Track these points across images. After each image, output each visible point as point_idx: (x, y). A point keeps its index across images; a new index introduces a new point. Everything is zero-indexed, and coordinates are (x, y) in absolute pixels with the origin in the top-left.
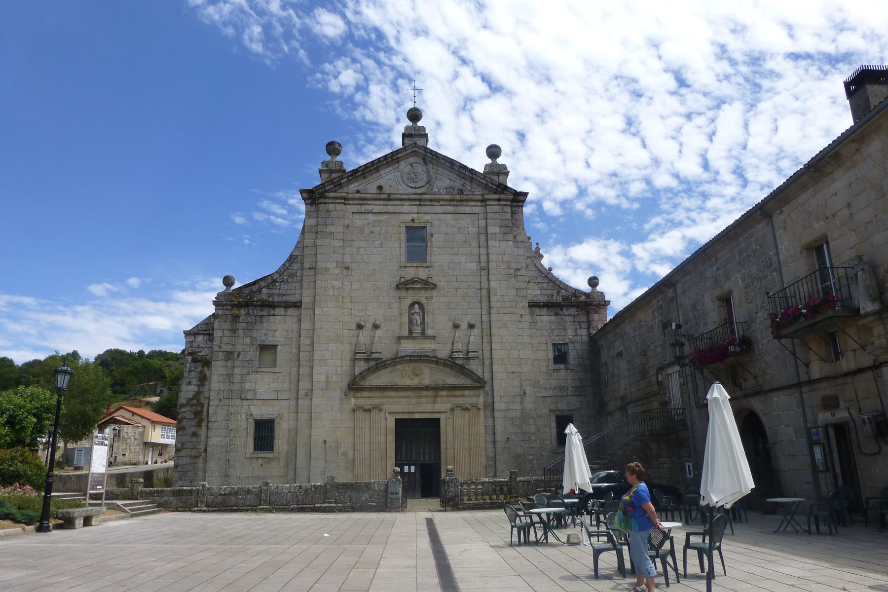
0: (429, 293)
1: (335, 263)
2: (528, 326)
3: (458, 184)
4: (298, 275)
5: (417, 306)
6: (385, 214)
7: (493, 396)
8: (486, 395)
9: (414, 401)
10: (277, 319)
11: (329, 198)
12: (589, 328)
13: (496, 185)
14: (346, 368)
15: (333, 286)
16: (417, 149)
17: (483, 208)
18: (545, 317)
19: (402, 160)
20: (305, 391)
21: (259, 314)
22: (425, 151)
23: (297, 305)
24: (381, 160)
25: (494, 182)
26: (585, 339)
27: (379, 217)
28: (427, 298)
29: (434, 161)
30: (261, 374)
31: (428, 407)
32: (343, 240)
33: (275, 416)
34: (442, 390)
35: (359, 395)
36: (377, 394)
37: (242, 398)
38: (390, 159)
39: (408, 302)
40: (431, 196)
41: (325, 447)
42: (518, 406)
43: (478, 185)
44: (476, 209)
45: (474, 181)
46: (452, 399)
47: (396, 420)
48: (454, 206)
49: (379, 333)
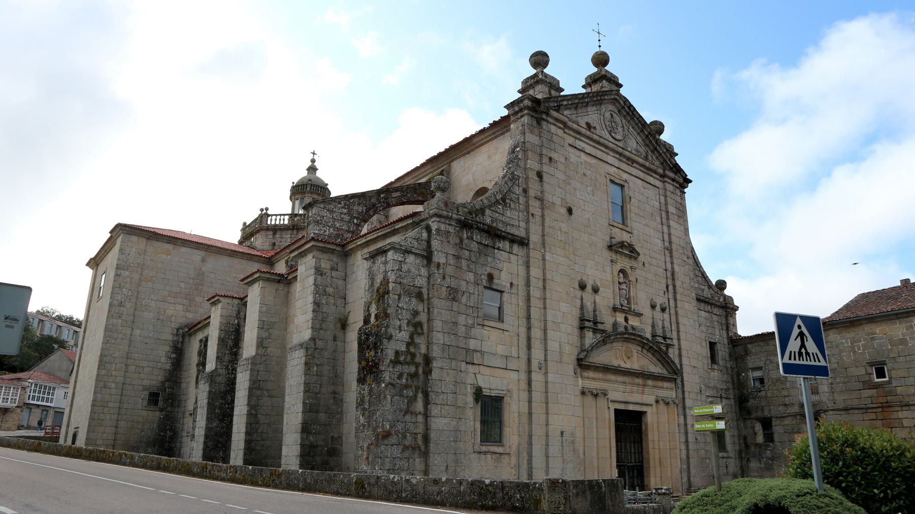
7: (683, 392)
10: (501, 254)
14: (575, 339)
20: (538, 361)
22: (624, 102)
23: (523, 242)
25: (672, 160)
26: (726, 341)
28: (631, 268)
29: (628, 118)
31: (636, 398)
33: (504, 392)
36: (600, 375)
37: (468, 361)
39: (618, 267)
41: (562, 442)
43: (657, 158)
44: (658, 183)
45: (655, 152)
48: (643, 172)
49: (598, 299)
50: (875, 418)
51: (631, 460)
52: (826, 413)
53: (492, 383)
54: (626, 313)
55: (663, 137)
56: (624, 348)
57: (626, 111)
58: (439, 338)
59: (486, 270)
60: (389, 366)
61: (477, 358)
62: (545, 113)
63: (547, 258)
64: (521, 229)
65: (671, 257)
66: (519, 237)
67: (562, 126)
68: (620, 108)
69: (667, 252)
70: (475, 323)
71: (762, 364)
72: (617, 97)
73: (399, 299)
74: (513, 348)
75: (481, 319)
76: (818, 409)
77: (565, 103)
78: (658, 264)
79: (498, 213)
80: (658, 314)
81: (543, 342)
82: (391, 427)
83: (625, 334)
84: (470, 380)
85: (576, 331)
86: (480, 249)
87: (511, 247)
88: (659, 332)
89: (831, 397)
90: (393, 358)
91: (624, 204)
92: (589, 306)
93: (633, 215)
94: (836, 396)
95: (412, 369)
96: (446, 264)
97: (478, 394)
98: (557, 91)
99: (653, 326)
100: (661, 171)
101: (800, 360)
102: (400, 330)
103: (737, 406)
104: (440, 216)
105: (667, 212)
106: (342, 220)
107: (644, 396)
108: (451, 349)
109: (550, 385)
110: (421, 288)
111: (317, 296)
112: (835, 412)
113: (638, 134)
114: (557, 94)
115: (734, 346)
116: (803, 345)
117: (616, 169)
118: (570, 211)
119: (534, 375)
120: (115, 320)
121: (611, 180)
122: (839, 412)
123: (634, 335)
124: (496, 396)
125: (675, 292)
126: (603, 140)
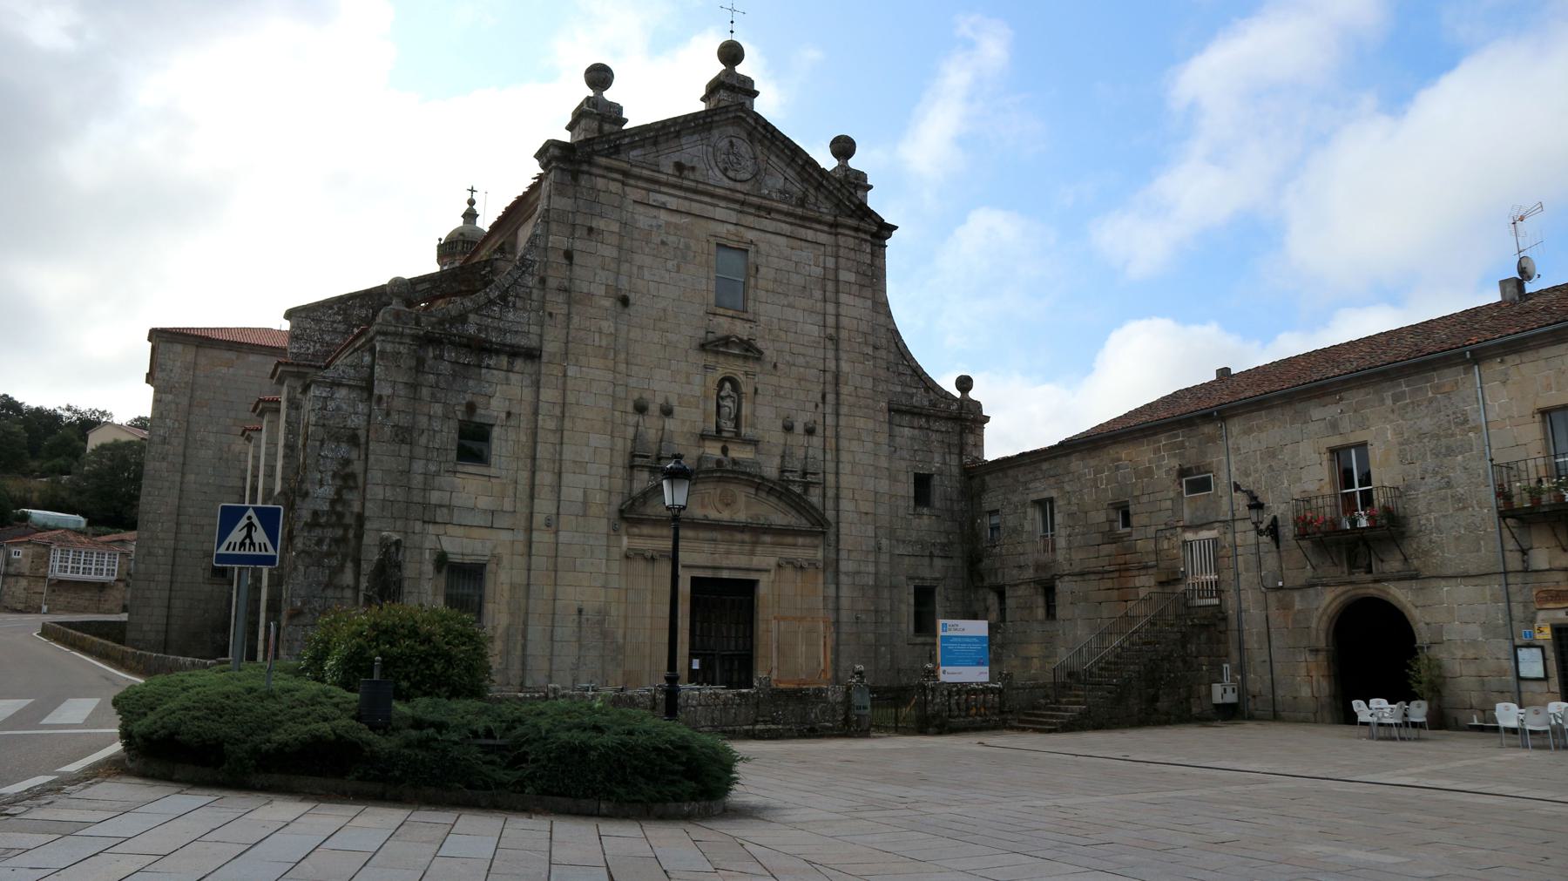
0: (751, 366)
1: (604, 287)
2: (887, 441)
3: (797, 188)
4: (534, 296)
5: (727, 385)
6: (685, 215)
7: (838, 551)
8: (826, 547)
9: (722, 548)
10: (493, 374)
11: (599, 166)
12: (961, 454)
13: (854, 205)
14: (618, 483)
15: (600, 329)
16: (744, 115)
17: (833, 237)
18: (906, 429)
19: (718, 127)
20: (545, 516)
23: (533, 355)
24: (689, 118)
25: (854, 199)
26: (955, 471)
27: (675, 219)
28: (746, 373)
29: (767, 142)
31: (742, 561)
32: (620, 248)
33: (486, 558)
34: (764, 533)
35: (636, 530)
37: (426, 519)
38: (701, 121)
39: (720, 374)
40: (760, 200)
42: (871, 569)
43: (826, 198)
44: (823, 238)
46: (778, 549)
48: (791, 224)
49: (670, 424)
50: (1111, 587)
52: (1062, 580)
53: (459, 544)
56: (719, 491)
57: (761, 133)
58: (376, 492)
59: (464, 398)
60: (302, 530)
61: (441, 515)
62: (585, 162)
63: (569, 373)
64: (531, 336)
65: (837, 350)
66: (523, 347)
69: (829, 345)
73: (322, 445)
75: (452, 464)
76: (1053, 573)
78: (807, 362)
79: (492, 318)
80: (799, 438)
81: (556, 489)
82: (304, 603)
83: (716, 471)
84: (430, 543)
87: (511, 363)
89: (1067, 556)
90: (309, 520)
92: (652, 435)
95: (340, 532)
96: (392, 396)
97: (441, 561)
98: (616, 124)
101: (250, 550)
102: (321, 484)
103: (966, 569)
104: (385, 334)
105: (837, 281)
106: (335, 331)
109: (561, 547)
110: (357, 429)
111: (290, 436)
112: (1070, 577)
113: (788, 165)
114: (616, 128)
115: (971, 478)
116: (249, 535)
117: (731, 227)
119: (536, 536)
120: (158, 464)
121: (718, 244)
122: (1075, 578)
124: (472, 563)
125: (838, 404)
126: (705, 187)
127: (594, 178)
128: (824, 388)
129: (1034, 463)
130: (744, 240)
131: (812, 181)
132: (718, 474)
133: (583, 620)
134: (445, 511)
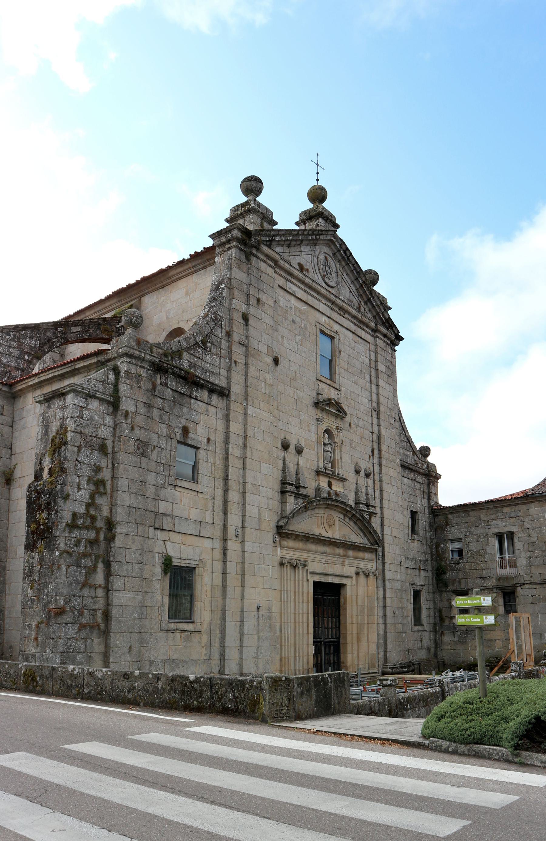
0: (340, 423)
7: (384, 564)
10: (198, 405)
14: (275, 504)
20: (235, 528)
21: (179, 390)
22: (340, 245)
25: (386, 314)
26: (427, 510)
27: (299, 305)
28: (337, 428)
29: (343, 263)
30: (181, 490)
31: (336, 569)
33: (196, 563)
36: (300, 545)
37: (157, 526)
43: (370, 310)
44: (369, 338)
45: (368, 304)
47: (316, 584)
48: (355, 324)
51: (328, 636)
52: (522, 587)
54: (330, 477)
55: (376, 288)
56: (326, 515)
57: (341, 255)
59: (180, 423)
60: (64, 531)
62: (256, 247)
64: (221, 377)
65: (378, 418)
66: (219, 386)
67: (273, 265)
68: (336, 251)
69: (374, 413)
70: (167, 483)
71: (462, 536)
72: (333, 238)
73: (79, 451)
74: (208, 512)
75: (173, 479)
76: (515, 582)
77: (278, 238)
78: (364, 425)
79: (197, 358)
81: (241, 507)
82: (66, 602)
83: (327, 500)
84: (159, 548)
85: (277, 496)
86: (174, 398)
87: (210, 398)
88: (363, 499)
90: (69, 522)
91: (334, 358)
92: (292, 468)
93: (342, 370)
94: (534, 570)
95: (92, 535)
96: (135, 413)
99: (357, 493)
100: (373, 325)
102: (79, 489)
104: (131, 356)
105: (377, 370)
107: (345, 568)
108: (138, 513)
109: (247, 555)
110: (106, 439)
113: (352, 282)
114: (270, 227)
115: (435, 516)
117: (327, 319)
118: (276, 361)
119: (229, 543)
122: (535, 586)
123: (337, 501)
124: (187, 567)
125: (380, 457)
127: (259, 261)
128: (373, 446)
129: (495, 508)
130: (333, 330)
131: (364, 297)
132: (329, 503)
133: (260, 616)
134: (169, 519)
